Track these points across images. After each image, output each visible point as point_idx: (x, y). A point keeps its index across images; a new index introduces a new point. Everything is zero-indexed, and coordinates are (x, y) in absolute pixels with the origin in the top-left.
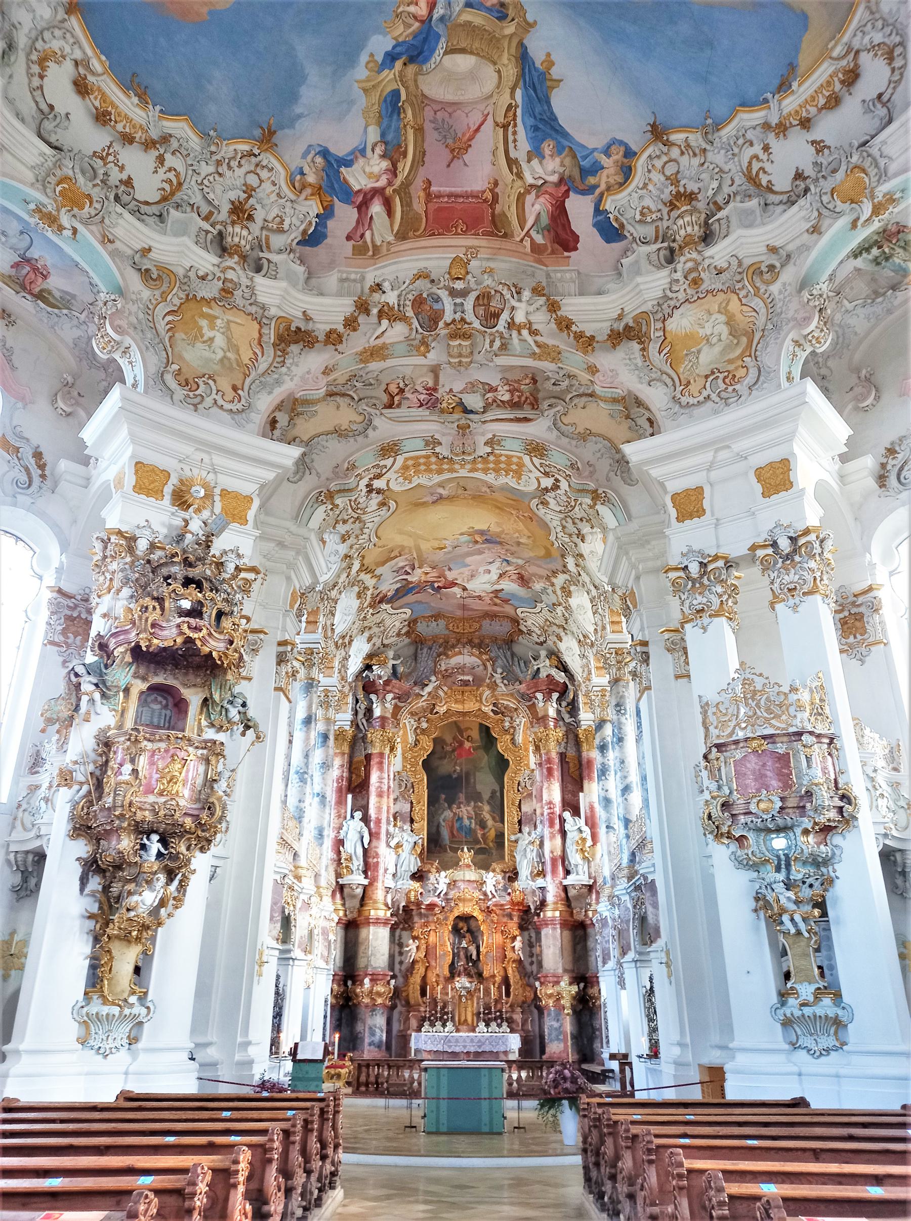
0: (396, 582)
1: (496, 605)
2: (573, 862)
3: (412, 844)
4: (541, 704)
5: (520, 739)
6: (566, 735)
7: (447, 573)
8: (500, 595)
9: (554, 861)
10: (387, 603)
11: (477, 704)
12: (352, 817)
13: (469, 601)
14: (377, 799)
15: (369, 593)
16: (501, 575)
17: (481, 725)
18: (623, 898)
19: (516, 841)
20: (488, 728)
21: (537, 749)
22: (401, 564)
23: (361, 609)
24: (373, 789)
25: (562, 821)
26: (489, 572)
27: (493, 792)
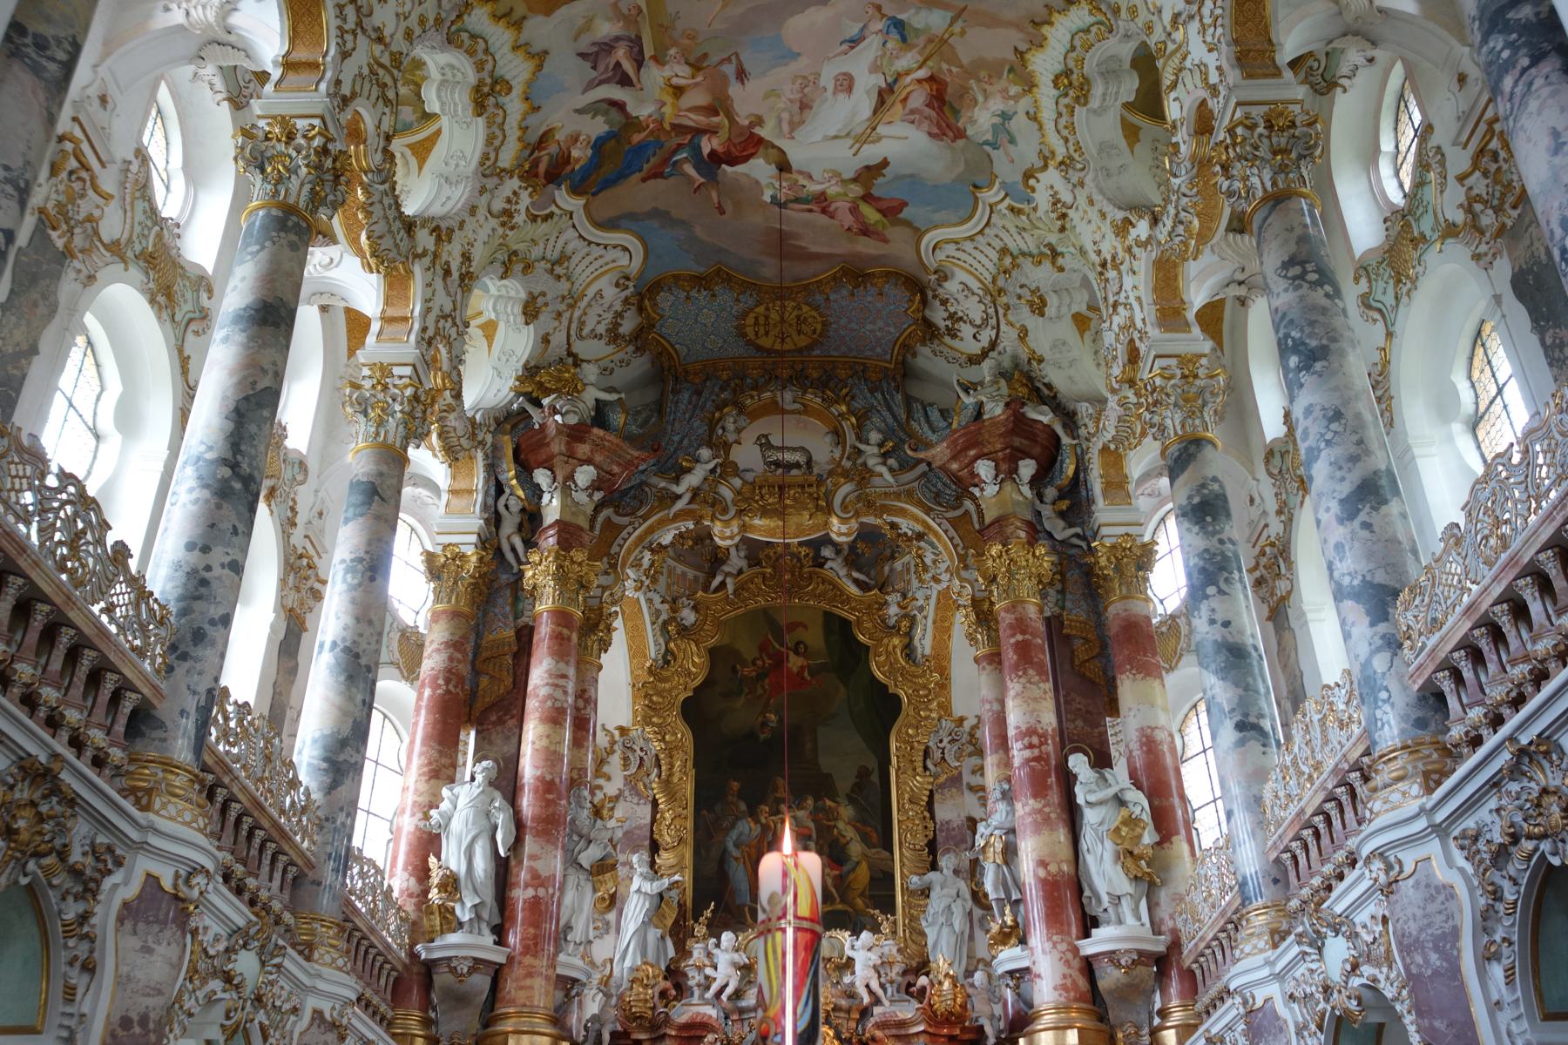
0: (592, 109)
1: (866, 231)
2: (1102, 887)
3: (656, 900)
4: (991, 490)
5: (924, 642)
6: (1061, 571)
7: (734, 90)
8: (880, 188)
9: (1051, 887)
10: (576, 191)
11: (820, 518)
12: (473, 779)
13: (795, 215)
14: (542, 729)
15: (514, 105)
16: (883, 98)
17: (828, 616)
18: (1409, 858)
19: (925, 892)
20: (845, 623)
21: (984, 615)
22: (606, 29)
23: (489, 170)
24: (532, 704)
25: (1067, 780)
26: (846, 84)
27: (863, 774)
